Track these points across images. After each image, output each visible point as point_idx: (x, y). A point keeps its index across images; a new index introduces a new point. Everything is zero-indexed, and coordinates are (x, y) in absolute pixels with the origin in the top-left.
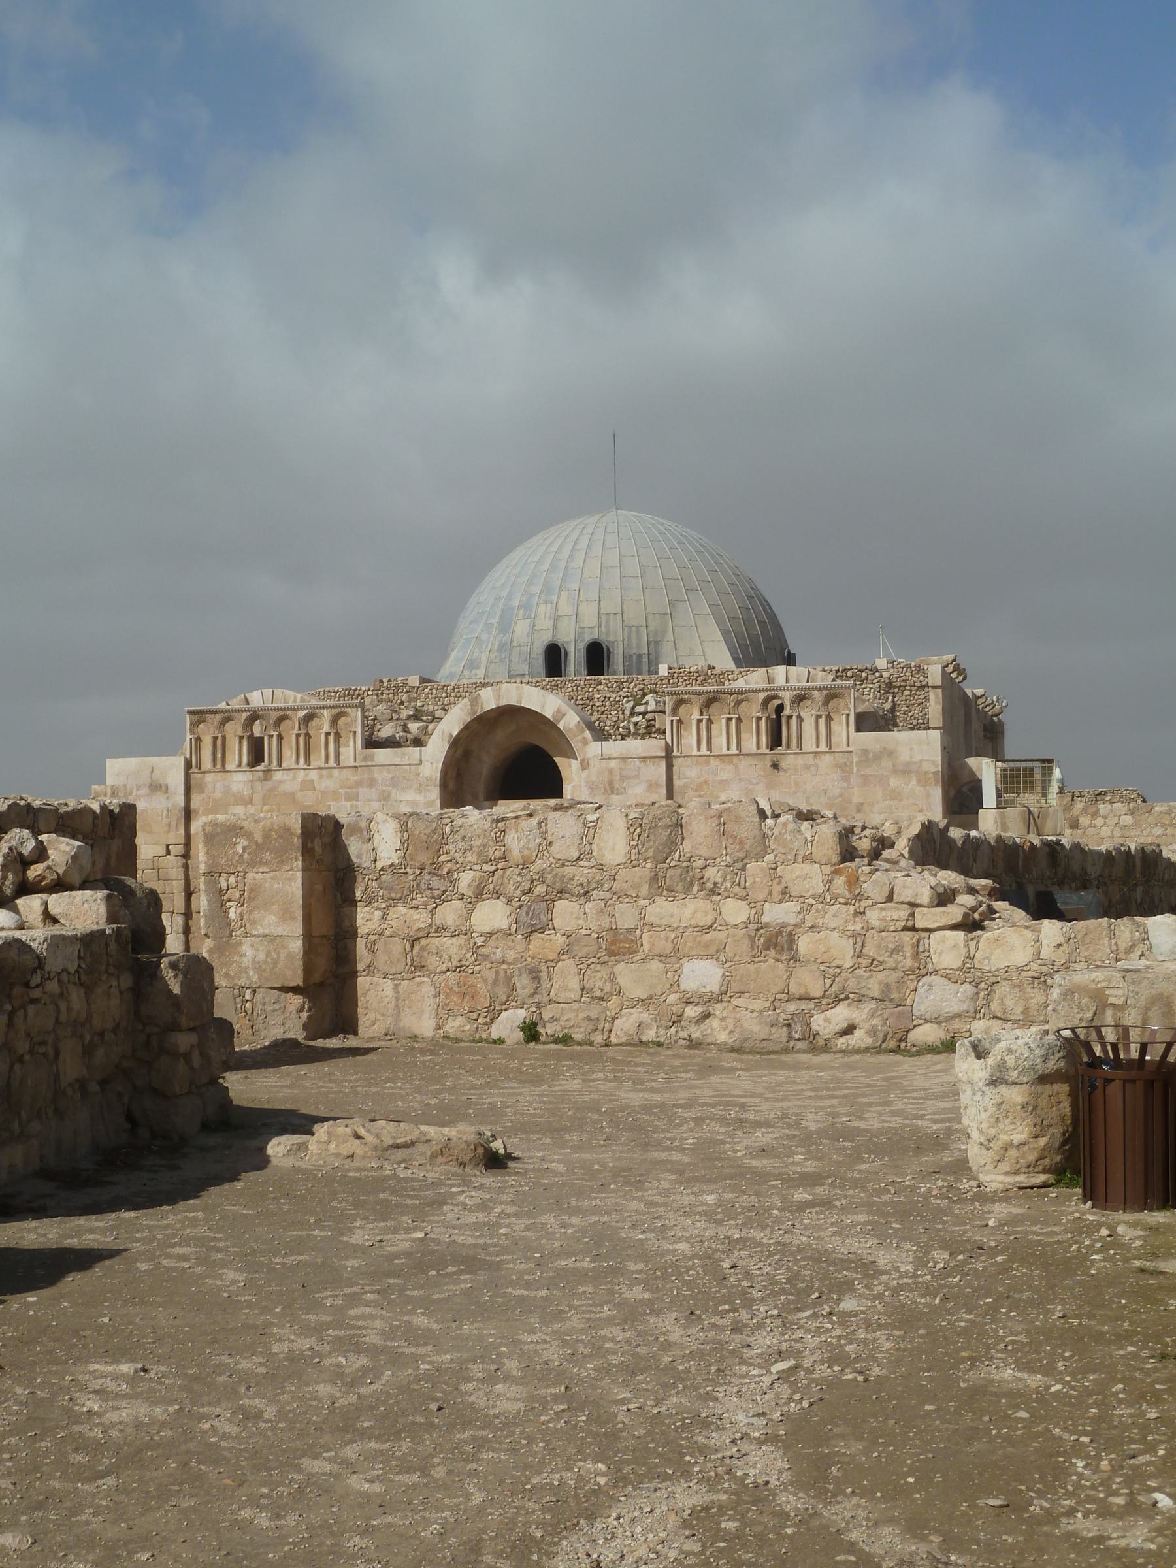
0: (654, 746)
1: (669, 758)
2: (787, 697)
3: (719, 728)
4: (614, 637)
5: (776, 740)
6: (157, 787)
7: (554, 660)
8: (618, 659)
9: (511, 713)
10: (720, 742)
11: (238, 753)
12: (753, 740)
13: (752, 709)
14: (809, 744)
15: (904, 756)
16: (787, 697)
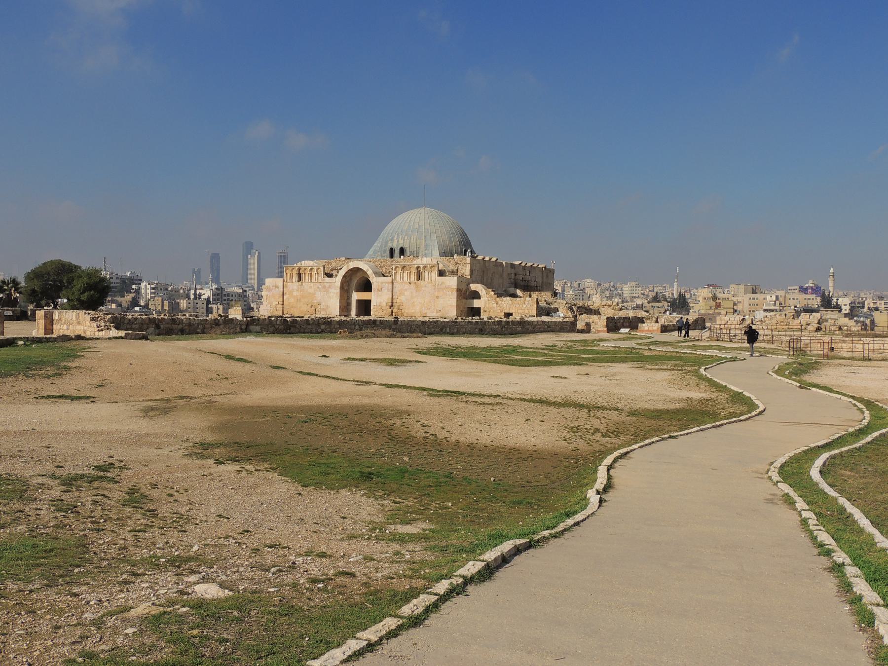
0: (389, 279)
1: (393, 283)
2: (422, 266)
3: (405, 274)
4: (406, 246)
5: (419, 278)
6: (277, 287)
7: (392, 251)
8: (408, 253)
9: (357, 270)
10: (405, 278)
11: (295, 278)
12: (413, 278)
13: (414, 270)
14: (426, 280)
15: (448, 284)
16: (422, 266)
